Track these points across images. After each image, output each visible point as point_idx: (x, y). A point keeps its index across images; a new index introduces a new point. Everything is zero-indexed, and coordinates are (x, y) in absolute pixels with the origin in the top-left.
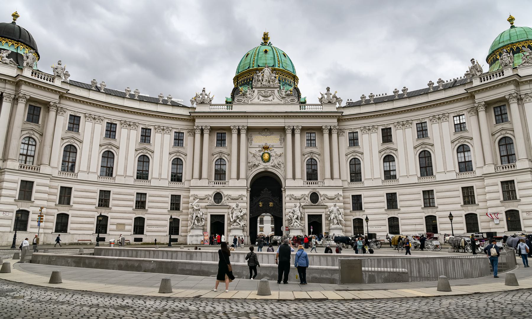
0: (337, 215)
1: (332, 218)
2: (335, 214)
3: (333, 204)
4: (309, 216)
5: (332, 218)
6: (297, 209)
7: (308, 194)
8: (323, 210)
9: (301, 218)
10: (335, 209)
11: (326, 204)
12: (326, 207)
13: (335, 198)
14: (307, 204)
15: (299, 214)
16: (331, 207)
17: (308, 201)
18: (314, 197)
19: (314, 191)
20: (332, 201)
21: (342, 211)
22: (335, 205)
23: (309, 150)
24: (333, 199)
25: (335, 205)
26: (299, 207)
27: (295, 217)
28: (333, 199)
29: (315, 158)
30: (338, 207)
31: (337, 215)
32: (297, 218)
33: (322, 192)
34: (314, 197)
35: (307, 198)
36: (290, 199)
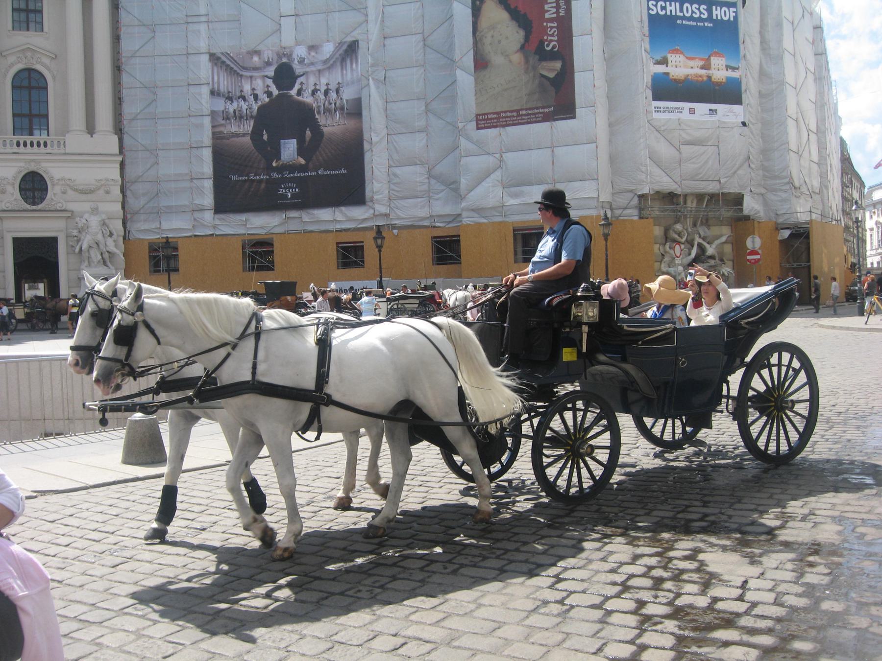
0: (100, 237)
3: (87, 206)
4: (16, 240)
5: (85, 247)
7: (15, 178)
10: (94, 222)
11: (71, 206)
12: (71, 216)
13: (98, 189)
17: (13, 197)
18: (33, 187)
19: (33, 167)
20: (89, 197)
23: (23, 38)
24: (91, 192)
28: (91, 192)
29: (38, 67)
30: (104, 216)
31: (100, 237)
33: (55, 172)
34: (33, 187)
35: (9, 189)
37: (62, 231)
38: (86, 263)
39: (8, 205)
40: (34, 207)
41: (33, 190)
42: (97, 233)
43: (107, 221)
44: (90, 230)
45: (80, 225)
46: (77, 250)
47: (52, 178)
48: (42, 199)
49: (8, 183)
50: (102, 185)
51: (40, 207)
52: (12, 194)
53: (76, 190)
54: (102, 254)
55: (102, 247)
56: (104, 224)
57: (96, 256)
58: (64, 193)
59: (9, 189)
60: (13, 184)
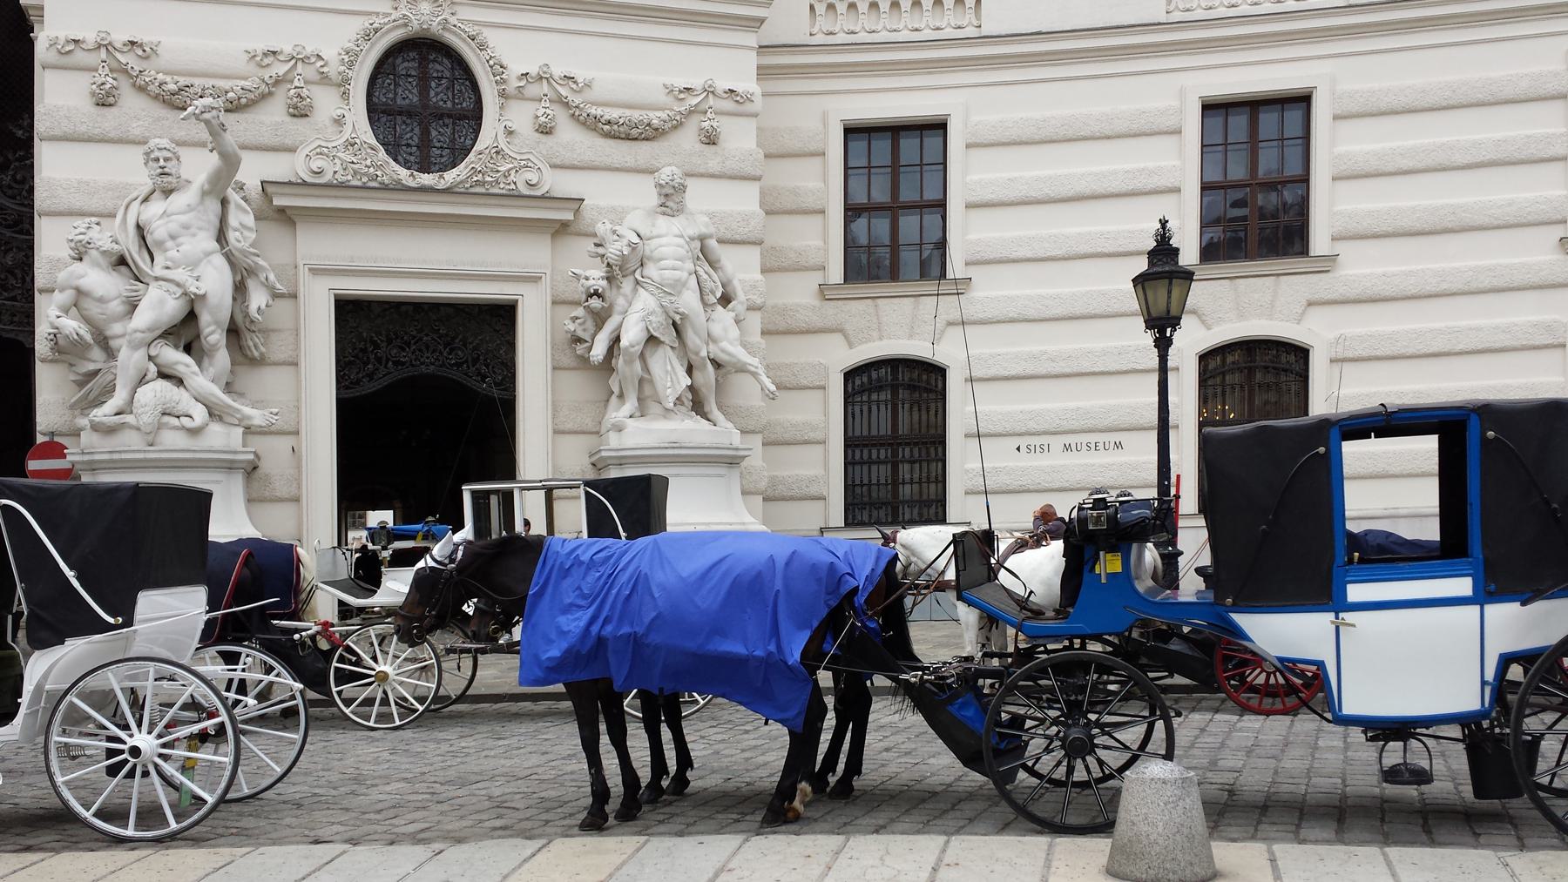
0: (689, 301)
1: (632, 335)
2: (670, 289)
4: (349, 311)
5: (632, 335)
6: (181, 224)
8: (530, 254)
9: (234, 332)
10: (669, 241)
11: (566, 184)
12: (563, 224)
14: (332, 170)
15: (215, 281)
16: (619, 215)
17: (339, 133)
20: (641, 153)
21: (742, 267)
22: (670, 199)
24: (651, 134)
25: (670, 199)
26: (219, 188)
27: (144, 317)
28: (651, 134)
30: (701, 225)
31: (689, 301)
32: (185, 331)
35: (326, 103)
36: (104, 101)
37: (534, 279)
38: (630, 405)
39: (316, 164)
40: (427, 179)
41: (425, 116)
42: (679, 285)
43: (712, 243)
44: (651, 270)
45: (614, 249)
46: (599, 351)
47: (498, 69)
48: (458, 153)
49: (324, 79)
50: (691, 112)
51: (451, 176)
52: (339, 121)
53: (593, 124)
54: (690, 370)
55: (692, 339)
56: (705, 255)
57: (670, 376)
58: (545, 130)
59: (326, 103)
60: (344, 82)
